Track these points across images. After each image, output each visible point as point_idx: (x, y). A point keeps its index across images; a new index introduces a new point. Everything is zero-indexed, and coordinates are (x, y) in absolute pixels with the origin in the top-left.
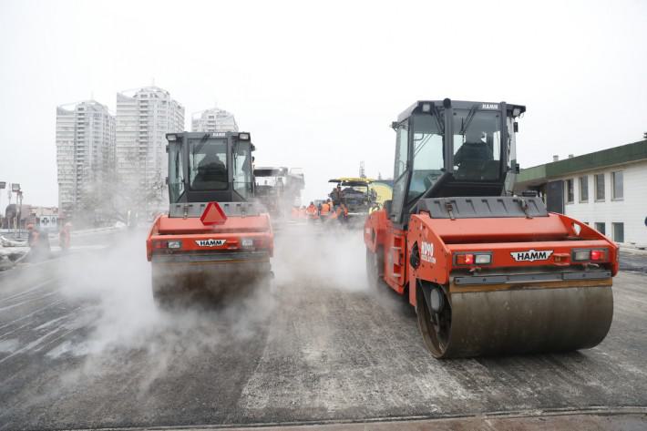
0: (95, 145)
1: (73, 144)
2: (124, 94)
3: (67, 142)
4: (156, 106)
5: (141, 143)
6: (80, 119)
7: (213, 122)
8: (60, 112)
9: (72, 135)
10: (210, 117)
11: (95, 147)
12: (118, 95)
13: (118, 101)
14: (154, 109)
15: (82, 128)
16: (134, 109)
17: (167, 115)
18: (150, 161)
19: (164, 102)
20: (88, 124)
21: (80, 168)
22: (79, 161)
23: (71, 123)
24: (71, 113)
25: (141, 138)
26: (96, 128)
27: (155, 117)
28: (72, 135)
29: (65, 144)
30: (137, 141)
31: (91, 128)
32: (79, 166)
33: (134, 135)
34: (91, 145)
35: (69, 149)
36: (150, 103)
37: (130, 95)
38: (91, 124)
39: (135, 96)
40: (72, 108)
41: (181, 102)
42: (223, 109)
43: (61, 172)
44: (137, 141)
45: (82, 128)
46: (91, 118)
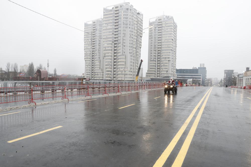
0: (100, 40)
1: (90, 41)
2: (108, 8)
3: (88, 39)
4: (123, 12)
5: (115, 35)
6: (94, 27)
7: (161, 22)
8: (86, 25)
9: (90, 36)
10: (159, 20)
11: (100, 41)
12: (104, 9)
13: (104, 13)
14: (122, 14)
15: (95, 32)
16: (112, 16)
17: (129, 17)
18: (119, 45)
19: (128, 9)
20: (97, 30)
21: (93, 52)
22: (93, 49)
23: (90, 30)
24: (90, 25)
25: (115, 32)
26: (100, 31)
27: (122, 18)
28: (90, 36)
29: (87, 41)
30: (113, 34)
31: (98, 31)
32: (93, 51)
33: (111, 30)
34: (98, 40)
35: (89, 43)
36: (120, 11)
37: (111, 8)
38: (98, 29)
39: (113, 8)
40: (91, 23)
41: (139, 10)
42: (168, 15)
43: (86, 55)
44: (113, 34)
45: (95, 32)
46: (98, 26)
